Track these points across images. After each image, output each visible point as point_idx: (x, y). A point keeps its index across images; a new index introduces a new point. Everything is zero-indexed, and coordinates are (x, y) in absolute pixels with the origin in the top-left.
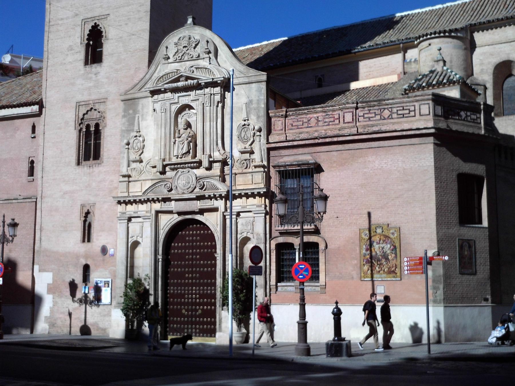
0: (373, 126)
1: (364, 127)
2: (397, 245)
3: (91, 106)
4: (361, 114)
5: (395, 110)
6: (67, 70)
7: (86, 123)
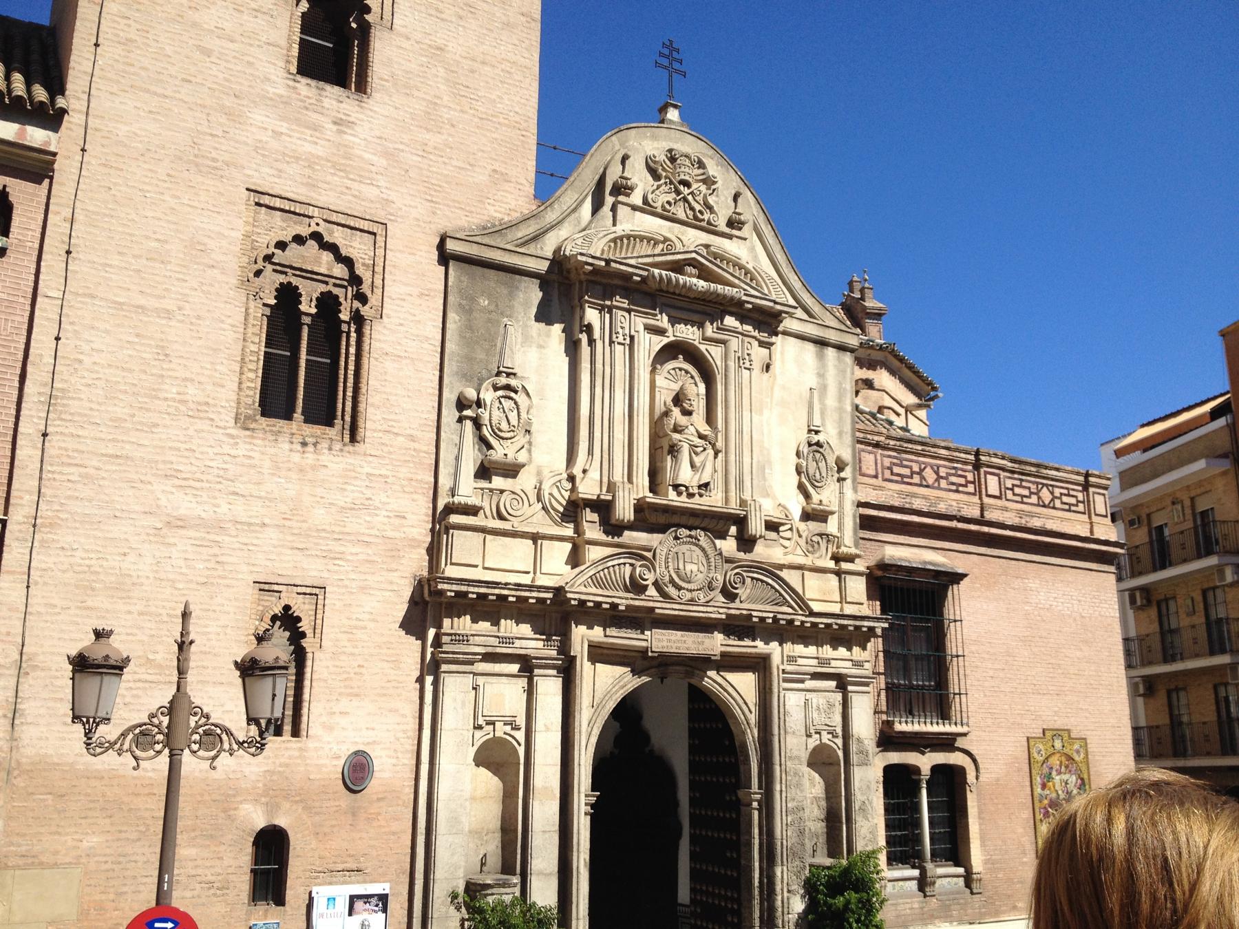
2: (1086, 777)
3: (314, 228)
7: (282, 279)
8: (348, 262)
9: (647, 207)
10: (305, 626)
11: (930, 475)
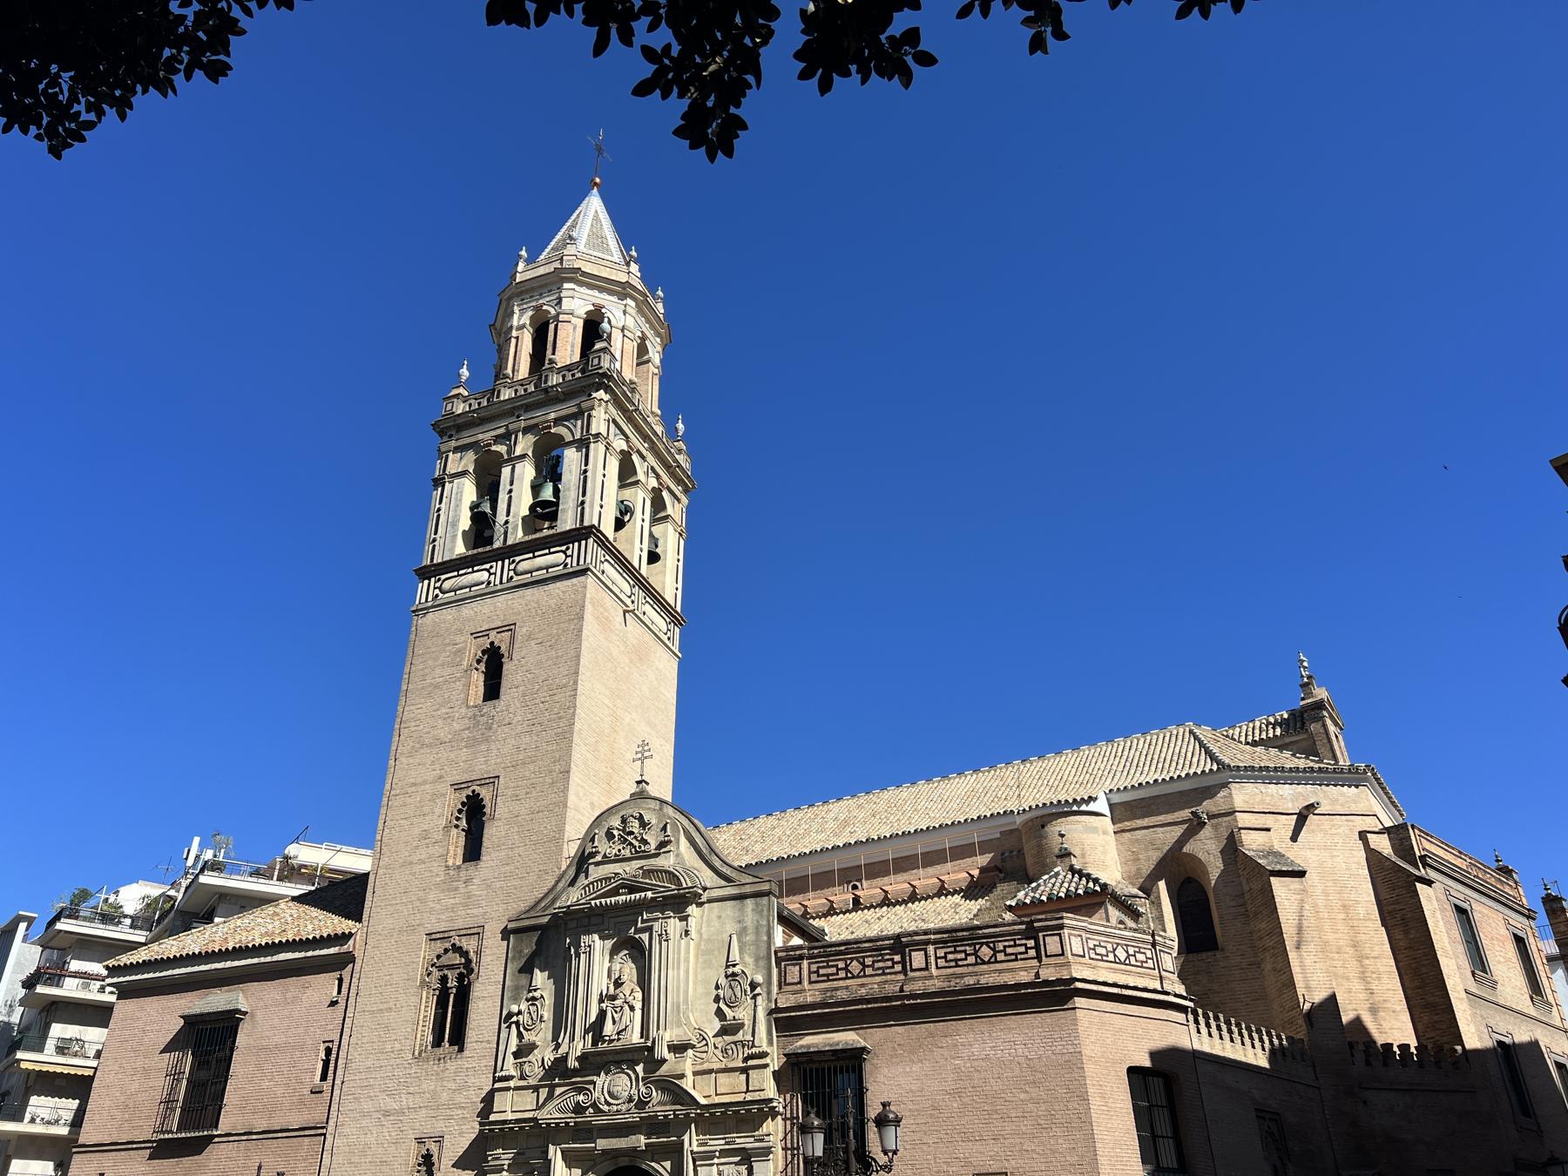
0: (962, 976)
1: (949, 977)
4: (941, 953)
5: (1000, 946)
6: (413, 874)
8: (465, 954)
9: (606, 860)
10: (435, 1159)
11: (855, 967)
